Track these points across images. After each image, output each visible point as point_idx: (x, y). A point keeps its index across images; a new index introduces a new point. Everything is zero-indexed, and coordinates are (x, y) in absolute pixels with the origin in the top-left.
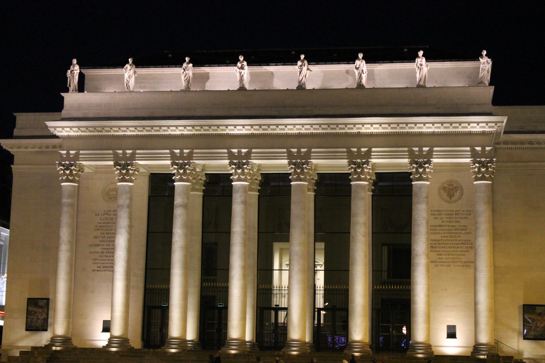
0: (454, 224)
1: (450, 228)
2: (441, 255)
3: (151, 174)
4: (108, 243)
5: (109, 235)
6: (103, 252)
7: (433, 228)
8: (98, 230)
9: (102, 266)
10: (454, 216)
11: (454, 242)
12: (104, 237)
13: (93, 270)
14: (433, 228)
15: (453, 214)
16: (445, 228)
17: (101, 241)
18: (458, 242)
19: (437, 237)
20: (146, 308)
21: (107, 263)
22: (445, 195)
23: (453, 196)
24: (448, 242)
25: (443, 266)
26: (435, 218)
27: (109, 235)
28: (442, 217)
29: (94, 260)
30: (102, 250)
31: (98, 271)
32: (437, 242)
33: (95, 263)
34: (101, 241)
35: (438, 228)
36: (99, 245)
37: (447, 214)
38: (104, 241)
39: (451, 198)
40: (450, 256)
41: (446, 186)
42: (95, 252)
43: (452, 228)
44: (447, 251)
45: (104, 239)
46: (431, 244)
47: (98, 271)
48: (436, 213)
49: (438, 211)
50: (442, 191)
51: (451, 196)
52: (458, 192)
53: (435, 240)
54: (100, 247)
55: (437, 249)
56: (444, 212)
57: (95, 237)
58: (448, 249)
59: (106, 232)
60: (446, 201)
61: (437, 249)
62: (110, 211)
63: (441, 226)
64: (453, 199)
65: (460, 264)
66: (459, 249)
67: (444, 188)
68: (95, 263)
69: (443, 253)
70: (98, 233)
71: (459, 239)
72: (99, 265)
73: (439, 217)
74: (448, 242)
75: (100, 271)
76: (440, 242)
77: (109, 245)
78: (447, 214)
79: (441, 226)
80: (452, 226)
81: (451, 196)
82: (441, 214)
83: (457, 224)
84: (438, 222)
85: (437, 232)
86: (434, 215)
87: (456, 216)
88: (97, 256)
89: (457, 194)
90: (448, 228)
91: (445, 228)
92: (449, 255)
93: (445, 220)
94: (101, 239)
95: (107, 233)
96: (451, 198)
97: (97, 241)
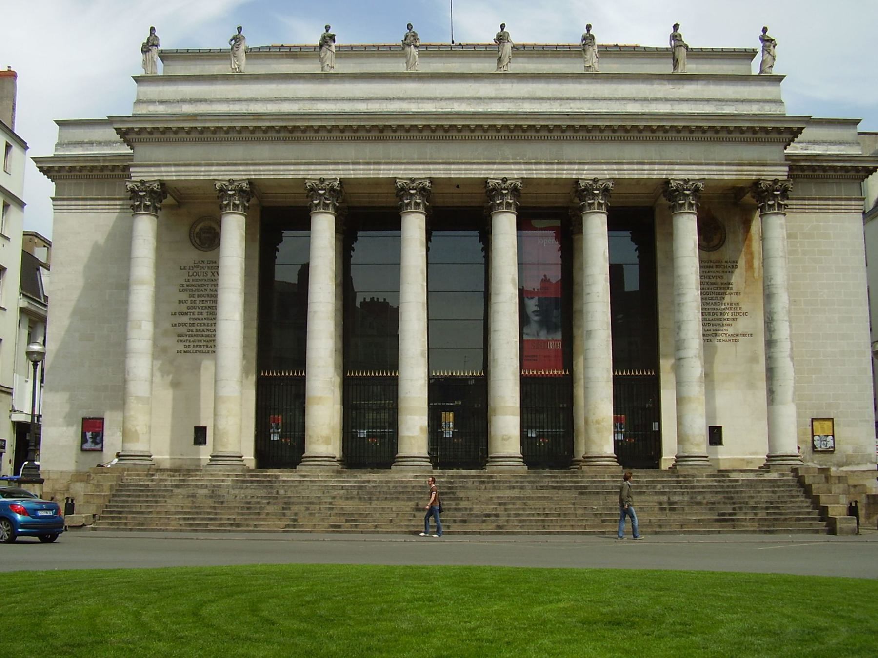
4: (200, 311)
5: (203, 299)
6: (193, 324)
8: (186, 290)
9: (192, 344)
12: (195, 302)
13: (178, 352)
15: (712, 267)
17: (188, 308)
21: (199, 341)
27: (203, 299)
29: (179, 336)
30: (192, 322)
31: (185, 352)
33: (181, 341)
34: (188, 308)
36: (186, 314)
38: (194, 308)
40: (711, 327)
42: (180, 324)
43: (712, 286)
45: (193, 305)
47: (185, 352)
54: (188, 317)
57: (180, 302)
59: (196, 293)
62: (203, 262)
68: (181, 341)
70: (184, 296)
72: (187, 344)
75: (189, 352)
77: (201, 314)
80: (712, 284)
83: (719, 280)
88: (183, 330)
94: (189, 304)
95: (198, 296)
97: (183, 308)
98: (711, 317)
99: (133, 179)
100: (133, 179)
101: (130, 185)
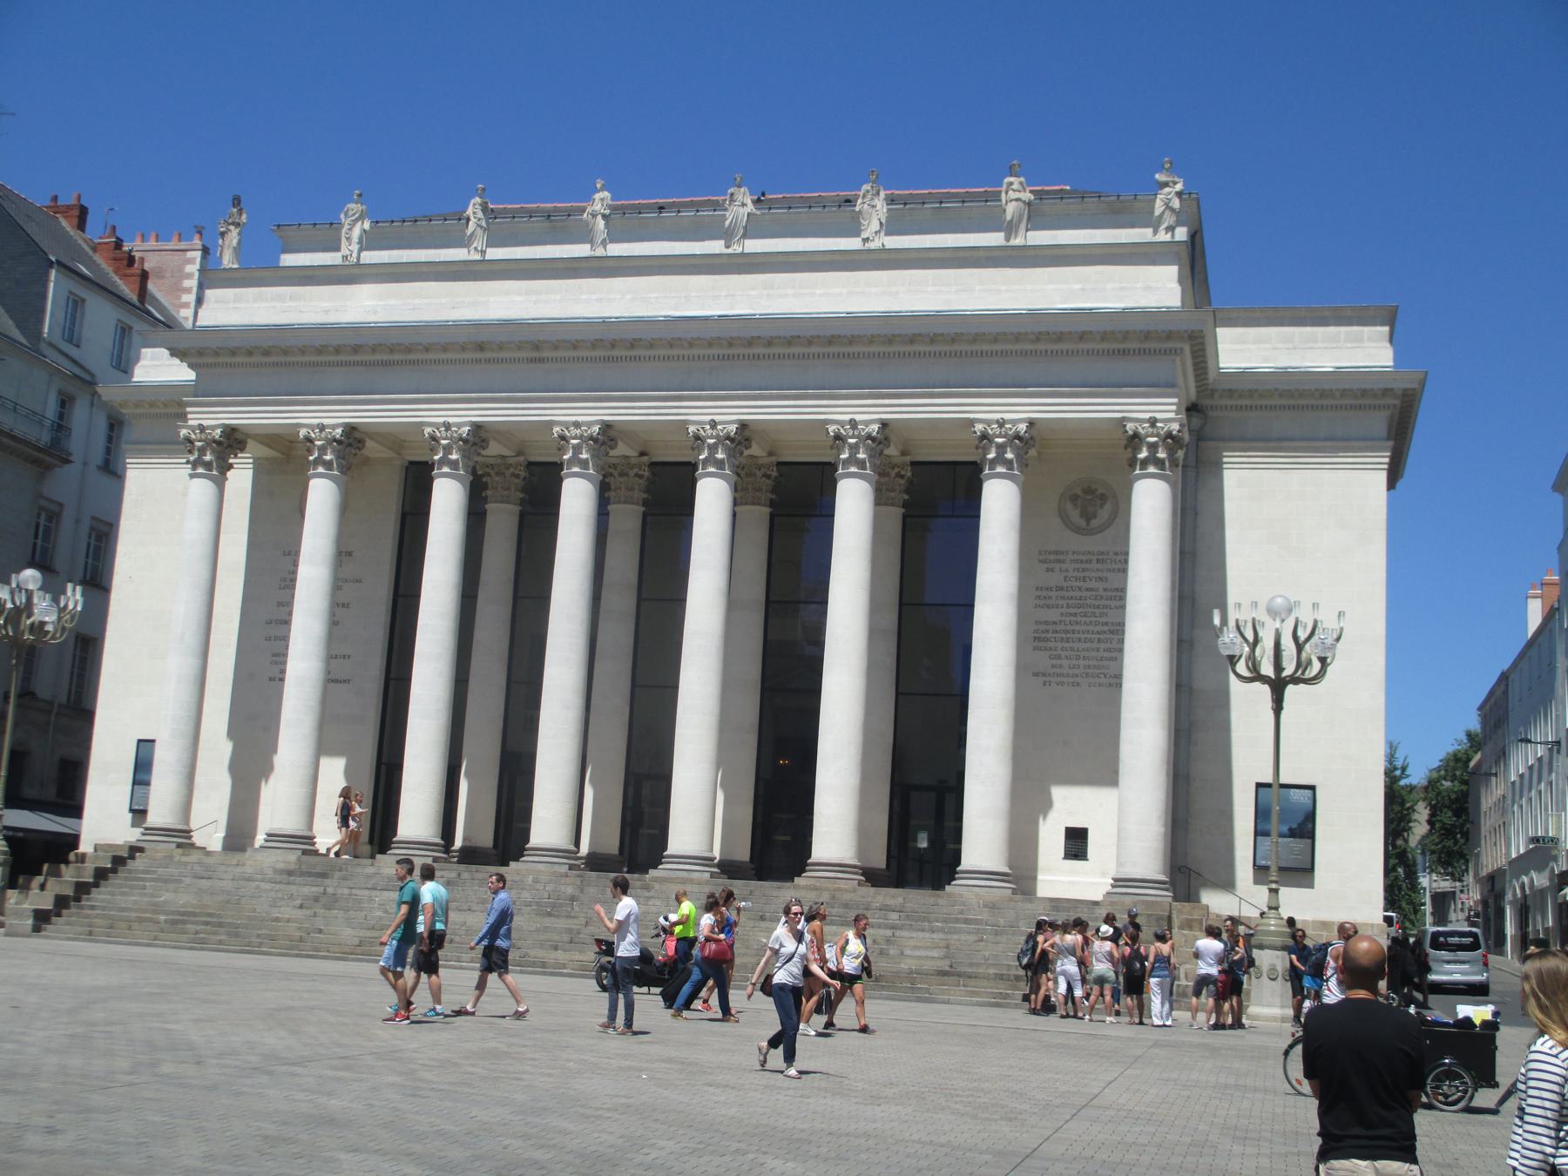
0: (1093, 584)
1: (1084, 594)
2: (1059, 657)
3: (412, 463)
7: (1044, 593)
10: (1095, 566)
11: (1091, 628)
14: (1044, 593)
15: (1090, 561)
16: (1071, 594)
18: (1100, 628)
19: (1053, 615)
20: (383, 768)
22: (1075, 516)
23: (1095, 516)
24: (1077, 628)
25: (1062, 683)
26: (1048, 570)
28: (1064, 566)
32: (1051, 627)
35: (1053, 594)
37: (1076, 561)
39: (1088, 521)
40: (1081, 662)
41: (1078, 491)
44: (1072, 649)
46: (1036, 631)
48: (1052, 557)
49: (1056, 553)
50: (1069, 506)
51: (1088, 516)
52: (1108, 506)
53: (1046, 623)
55: (1052, 645)
56: (1070, 557)
58: (1076, 645)
60: (1078, 530)
61: (1049, 644)
63: (1061, 589)
64: (1094, 523)
65: (1103, 680)
66: (1102, 646)
67: (1074, 498)
69: (1063, 654)
71: (1104, 620)
73: (1057, 566)
74: (1077, 628)
76: (1058, 628)
78: (1076, 561)
79: (1061, 589)
81: (1088, 516)
82: (1063, 562)
83: (1101, 585)
84: (1055, 579)
85: (1052, 602)
86: (1045, 562)
87: (1100, 566)
89: (1104, 514)
90: (1078, 594)
91: (1071, 594)
92: (1078, 657)
93: (1071, 574)
96: (1088, 521)
98: (1082, 646)
99: (191, 423)
100: (191, 423)
101: (184, 432)
